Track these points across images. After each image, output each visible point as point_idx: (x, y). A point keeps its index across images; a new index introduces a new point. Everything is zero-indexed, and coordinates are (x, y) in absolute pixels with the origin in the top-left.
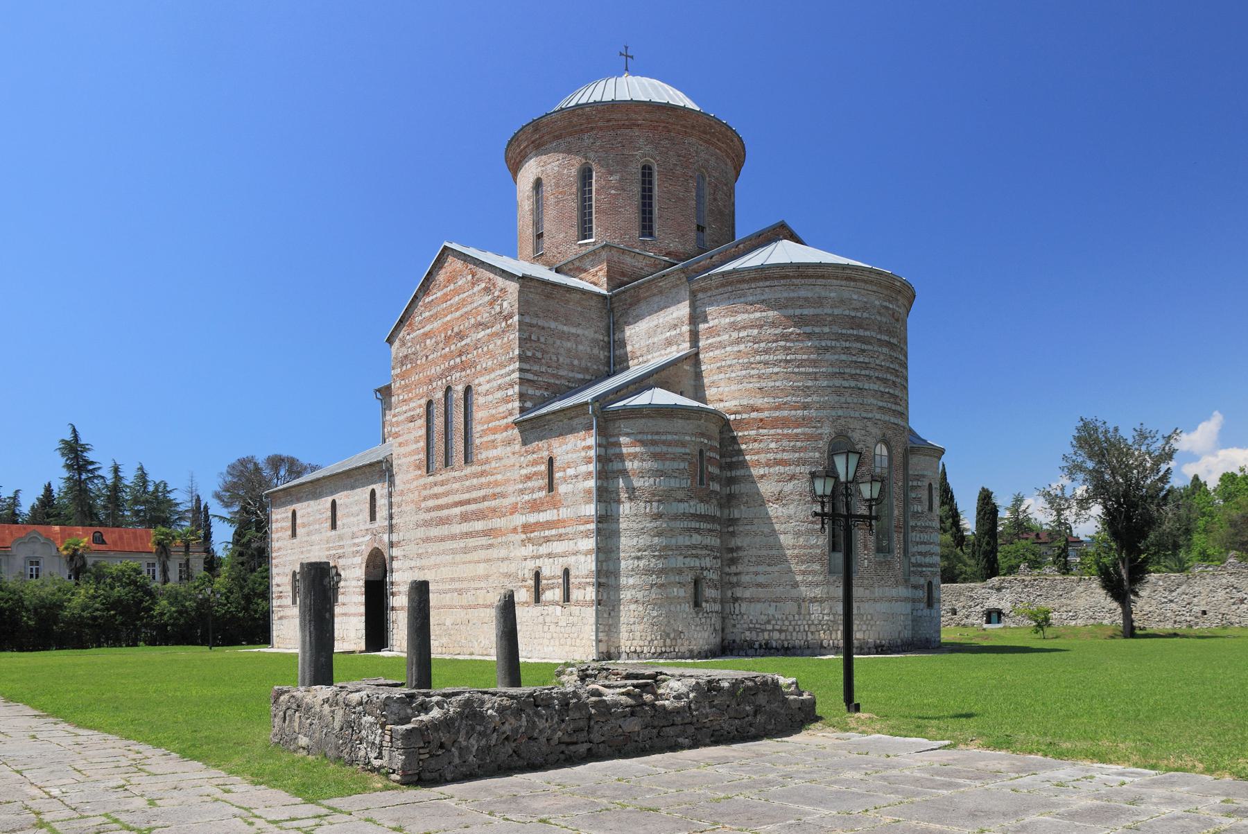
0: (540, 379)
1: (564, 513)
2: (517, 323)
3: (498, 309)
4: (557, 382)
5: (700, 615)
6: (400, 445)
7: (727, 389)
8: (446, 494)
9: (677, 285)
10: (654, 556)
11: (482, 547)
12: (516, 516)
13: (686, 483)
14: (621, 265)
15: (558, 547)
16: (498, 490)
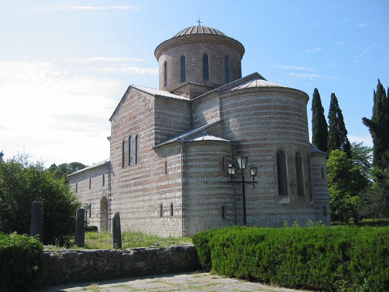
1: (171, 182)
2: (154, 112)
4: (170, 133)
5: (225, 221)
8: (129, 176)
9: (215, 96)
10: (205, 198)
13: (218, 170)
15: (168, 195)
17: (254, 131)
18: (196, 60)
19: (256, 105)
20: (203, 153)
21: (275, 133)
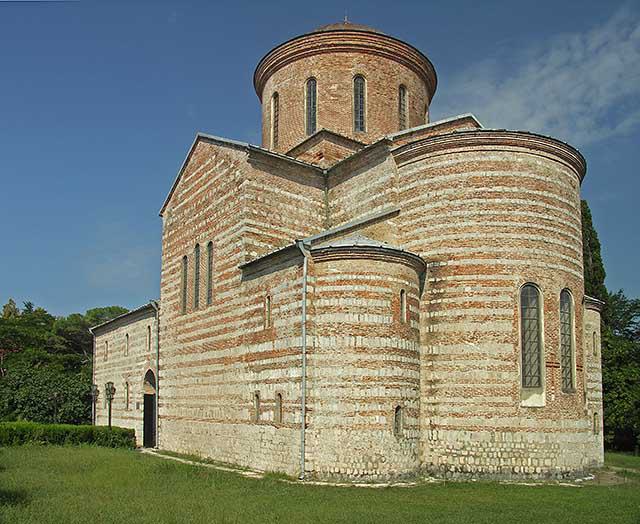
1: (279, 344)
3: (232, 178)
11: (217, 372)
13: (388, 319)
15: (274, 374)
16: (229, 325)
19: (476, 174)
20: (355, 277)
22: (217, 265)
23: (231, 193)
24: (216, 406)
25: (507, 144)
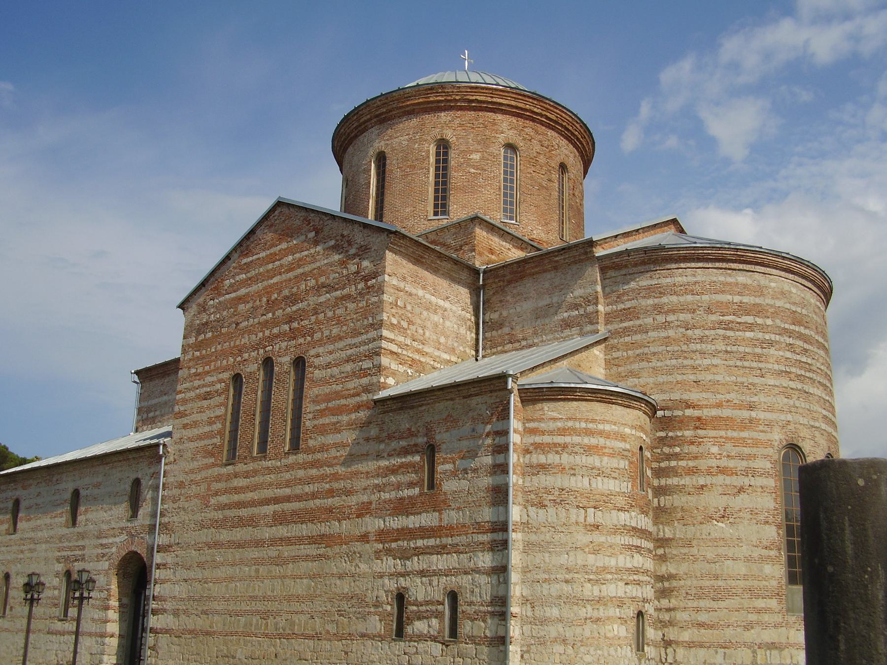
0: (405, 352)
1: (451, 517)
6: (185, 426)
7: (651, 380)
9: (581, 261)
10: (590, 580)
11: (307, 558)
12: (367, 519)
14: (490, 242)
15: (439, 562)
17: (718, 378)
18: (482, 158)
20: (583, 425)
21: (777, 390)
22: (311, 391)
23: (351, 290)
24: (302, 612)
25: (757, 264)
